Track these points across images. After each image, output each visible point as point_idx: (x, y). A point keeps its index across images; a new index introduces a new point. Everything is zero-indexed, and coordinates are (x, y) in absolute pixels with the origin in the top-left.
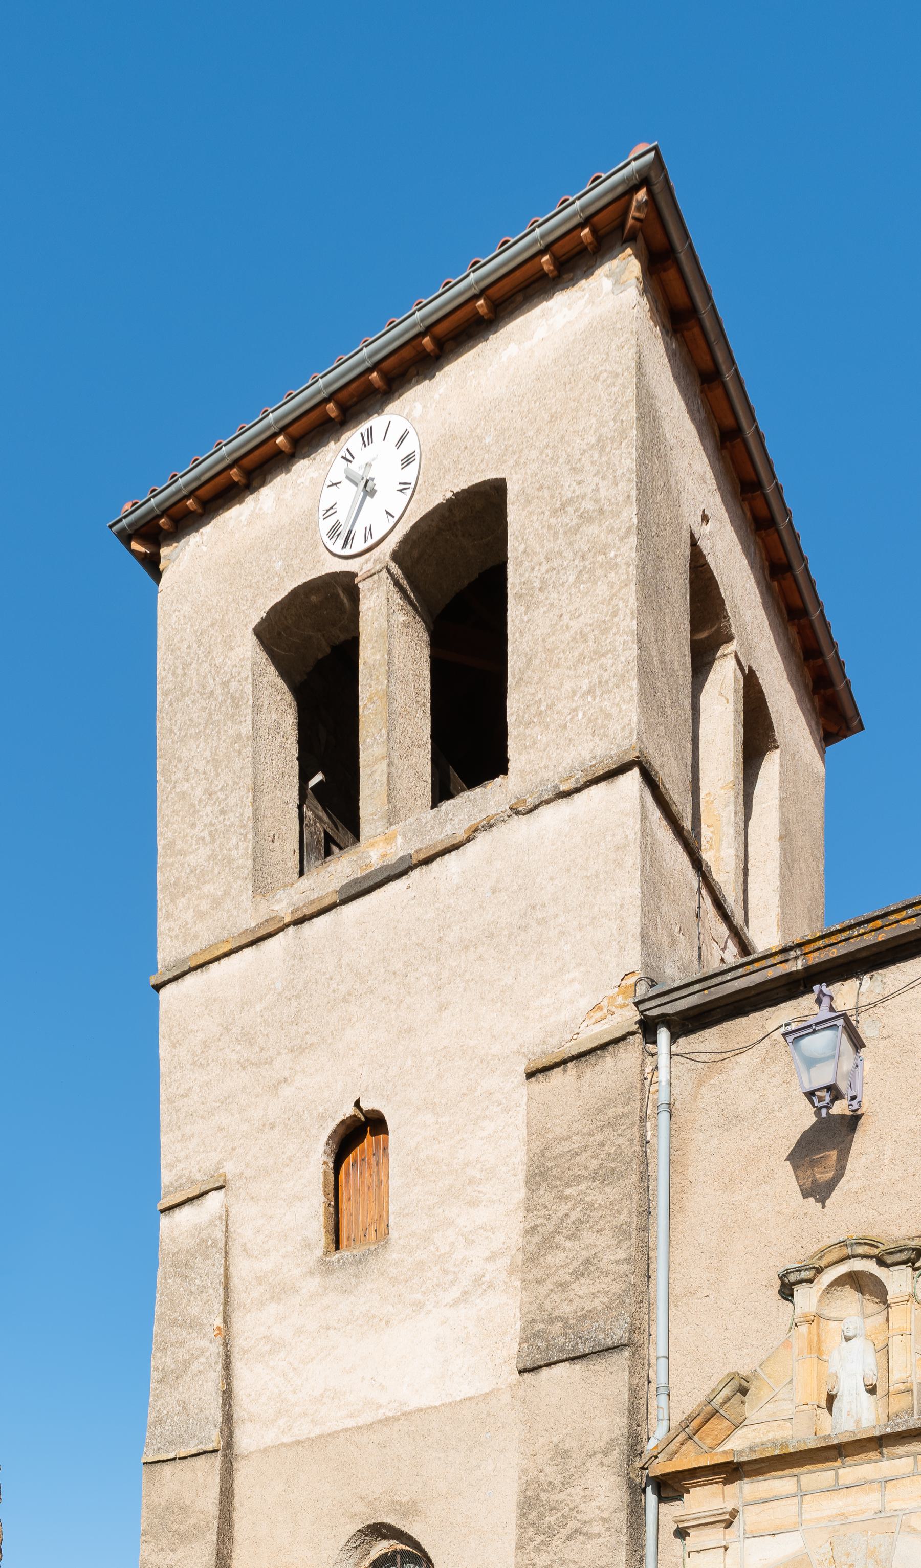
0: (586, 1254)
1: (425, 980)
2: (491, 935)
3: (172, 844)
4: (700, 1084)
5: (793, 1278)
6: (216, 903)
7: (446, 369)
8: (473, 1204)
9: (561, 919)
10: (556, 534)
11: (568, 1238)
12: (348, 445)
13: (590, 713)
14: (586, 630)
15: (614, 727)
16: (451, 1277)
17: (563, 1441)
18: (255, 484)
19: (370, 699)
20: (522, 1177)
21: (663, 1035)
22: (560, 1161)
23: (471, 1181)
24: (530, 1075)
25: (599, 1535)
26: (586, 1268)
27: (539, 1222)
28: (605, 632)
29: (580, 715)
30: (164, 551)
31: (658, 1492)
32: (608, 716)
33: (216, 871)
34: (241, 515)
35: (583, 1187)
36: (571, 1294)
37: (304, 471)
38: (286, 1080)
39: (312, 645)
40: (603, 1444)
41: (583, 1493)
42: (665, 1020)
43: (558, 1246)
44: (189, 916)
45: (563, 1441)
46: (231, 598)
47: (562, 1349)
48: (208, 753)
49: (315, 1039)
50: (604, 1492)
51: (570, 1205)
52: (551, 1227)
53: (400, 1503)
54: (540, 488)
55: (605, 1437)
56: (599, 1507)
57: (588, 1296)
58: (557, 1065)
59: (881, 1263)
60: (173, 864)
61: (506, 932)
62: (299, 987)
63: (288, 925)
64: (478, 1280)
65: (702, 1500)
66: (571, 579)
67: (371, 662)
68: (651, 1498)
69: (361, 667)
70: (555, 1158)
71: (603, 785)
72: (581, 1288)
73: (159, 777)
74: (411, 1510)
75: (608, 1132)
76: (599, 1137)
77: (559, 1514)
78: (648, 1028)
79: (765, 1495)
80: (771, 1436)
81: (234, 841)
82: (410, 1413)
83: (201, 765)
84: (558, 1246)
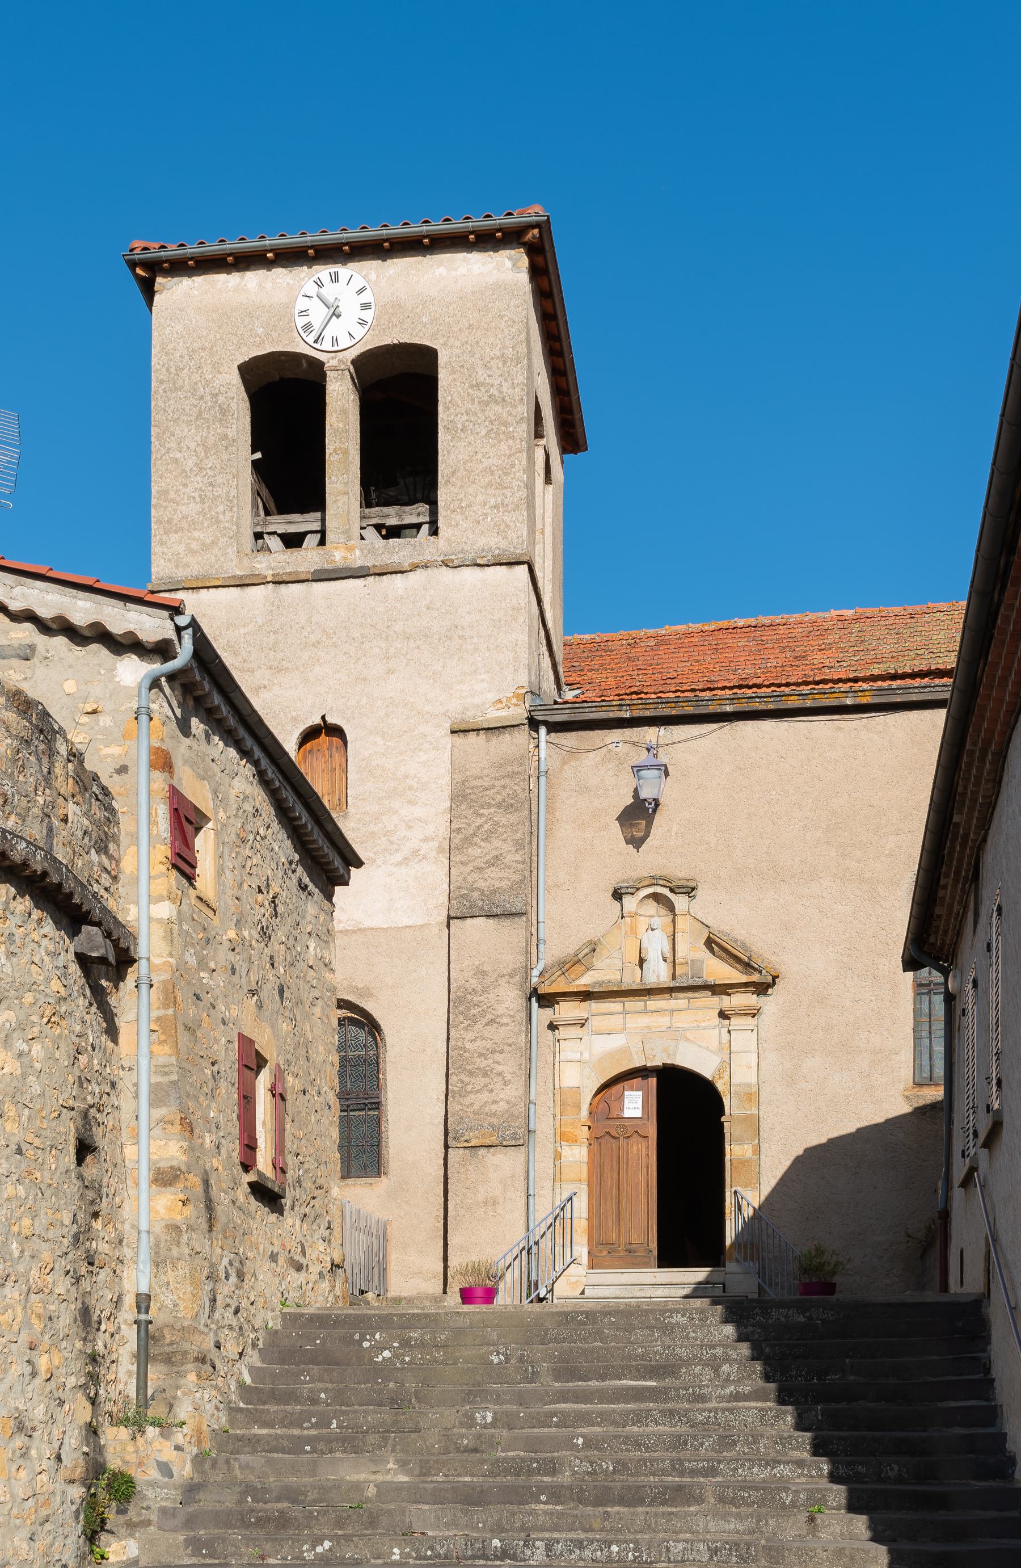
0: (495, 853)
1: (377, 650)
2: (426, 636)
3: (166, 492)
4: (564, 763)
5: (623, 891)
6: (205, 547)
7: (395, 260)
8: (411, 802)
9: (475, 640)
10: (473, 400)
11: (482, 840)
12: (319, 275)
13: (496, 520)
14: (493, 468)
15: (512, 535)
16: (396, 847)
18: (241, 266)
19: (335, 451)
20: (447, 793)
21: (543, 730)
22: (475, 791)
23: (410, 788)
24: (453, 732)
25: (507, 1025)
26: (495, 861)
27: (462, 826)
28: (506, 474)
29: (489, 519)
30: (159, 280)
31: (538, 1001)
32: (508, 526)
33: (206, 524)
34: (228, 282)
35: (492, 810)
37: (279, 273)
38: (265, 687)
39: (282, 397)
40: (509, 970)
42: (546, 723)
43: (475, 844)
44: (181, 548)
46: (219, 337)
47: (482, 909)
48: (198, 438)
49: (290, 666)
50: (509, 999)
51: (483, 820)
52: (471, 831)
53: (356, 987)
54: (462, 367)
55: (511, 967)
57: (494, 879)
58: (473, 730)
59: (672, 890)
60: (166, 507)
61: (436, 637)
62: (277, 626)
63: (268, 582)
64: (415, 852)
65: (566, 1010)
66: (483, 433)
67: (335, 426)
68: (535, 1004)
69: (328, 427)
70: (473, 788)
71: (504, 567)
72: (492, 873)
73: (153, 439)
74: (366, 992)
75: (507, 781)
76: (502, 782)
78: (534, 724)
79: (604, 1011)
80: (608, 977)
81: (221, 508)
82: (365, 929)
83: (193, 445)
84: (475, 844)
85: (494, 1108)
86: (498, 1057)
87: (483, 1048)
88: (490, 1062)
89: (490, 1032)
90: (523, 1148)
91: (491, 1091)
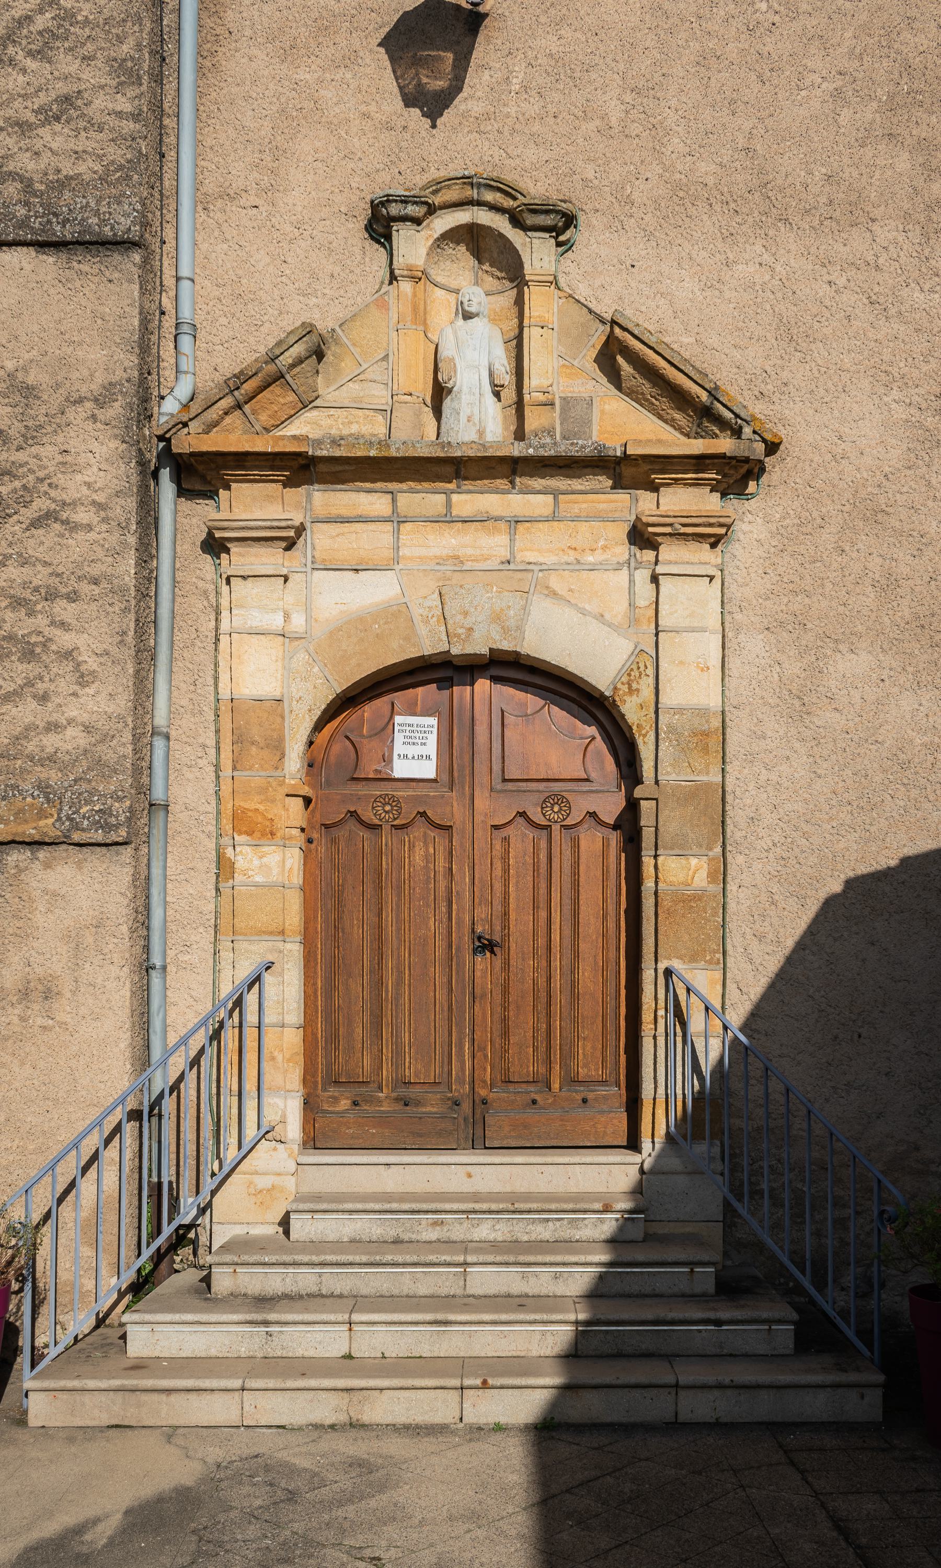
0: (62, 88)
11: (30, 54)
17: (25, 369)
25: (89, 528)
26: (65, 108)
36: (38, 145)
40: (95, 387)
41: (59, 458)
45: (25, 369)
50: (94, 464)
55: (100, 378)
56: (88, 485)
72: (54, 138)
77: (17, 484)
85: (51, 742)
86: (64, 610)
87: (25, 585)
88: (41, 621)
89: (41, 543)
90: (128, 851)
91: (44, 698)
